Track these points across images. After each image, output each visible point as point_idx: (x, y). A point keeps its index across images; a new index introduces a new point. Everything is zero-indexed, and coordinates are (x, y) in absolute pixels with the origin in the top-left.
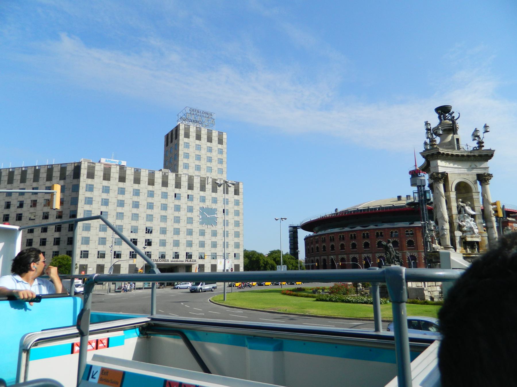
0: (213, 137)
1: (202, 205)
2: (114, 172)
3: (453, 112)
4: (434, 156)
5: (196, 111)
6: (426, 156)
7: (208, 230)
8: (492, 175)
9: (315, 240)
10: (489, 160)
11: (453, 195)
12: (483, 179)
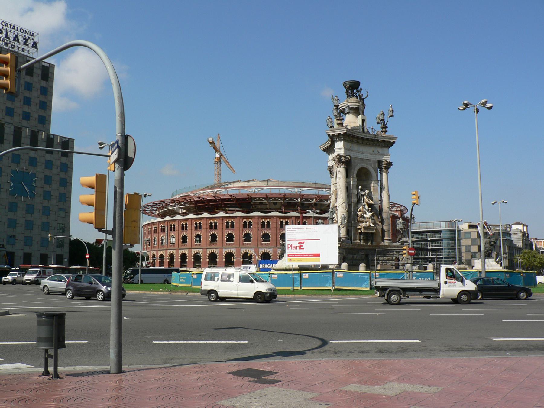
0: (35, 69)
1: (14, 167)
3: (361, 89)
4: (340, 137)
5: (12, 27)
6: (332, 135)
8: (392, 163)
9: (161, 228)
10: (391, 147)
12: (383, 167)
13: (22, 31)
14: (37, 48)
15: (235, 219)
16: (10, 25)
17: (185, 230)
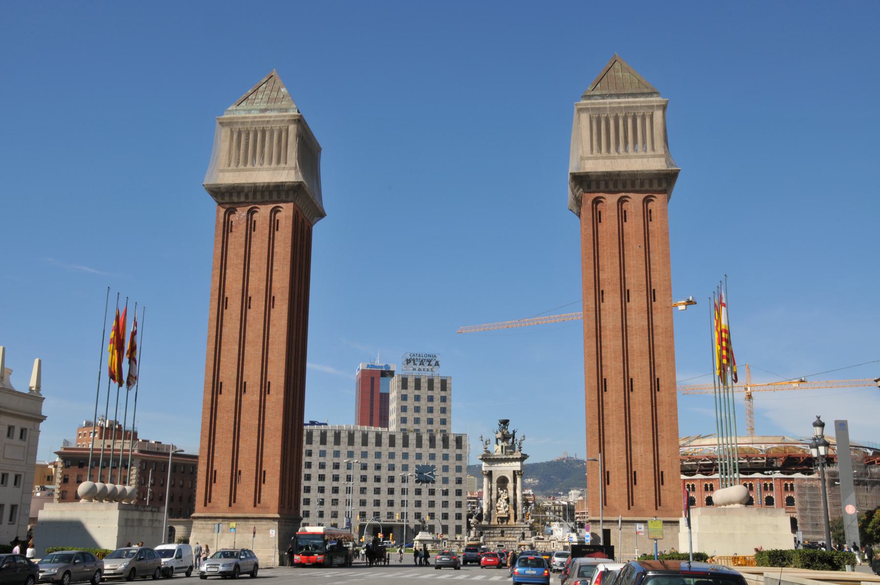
2: (330, 436)
7: (425, 488)
11: (494, 486)
13: (426, 356)
14: (438, 365)
15: (714, 481)
16: (417, 354)
17: (711, 490)
